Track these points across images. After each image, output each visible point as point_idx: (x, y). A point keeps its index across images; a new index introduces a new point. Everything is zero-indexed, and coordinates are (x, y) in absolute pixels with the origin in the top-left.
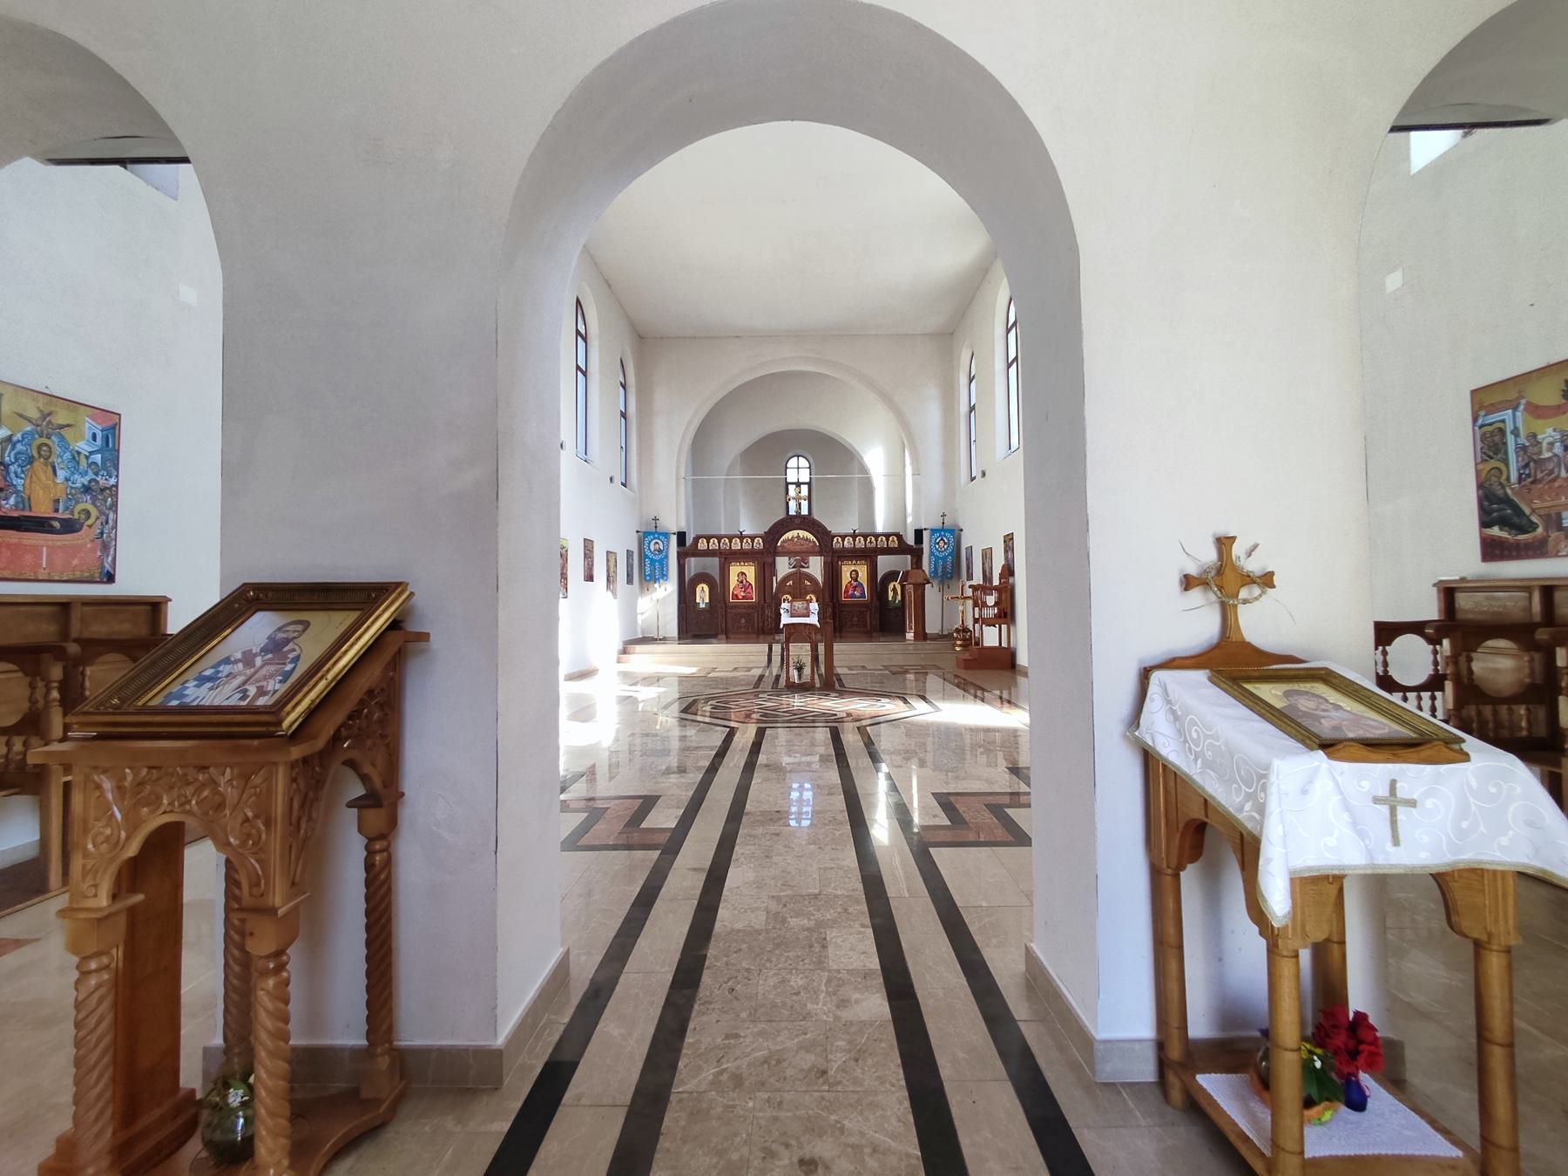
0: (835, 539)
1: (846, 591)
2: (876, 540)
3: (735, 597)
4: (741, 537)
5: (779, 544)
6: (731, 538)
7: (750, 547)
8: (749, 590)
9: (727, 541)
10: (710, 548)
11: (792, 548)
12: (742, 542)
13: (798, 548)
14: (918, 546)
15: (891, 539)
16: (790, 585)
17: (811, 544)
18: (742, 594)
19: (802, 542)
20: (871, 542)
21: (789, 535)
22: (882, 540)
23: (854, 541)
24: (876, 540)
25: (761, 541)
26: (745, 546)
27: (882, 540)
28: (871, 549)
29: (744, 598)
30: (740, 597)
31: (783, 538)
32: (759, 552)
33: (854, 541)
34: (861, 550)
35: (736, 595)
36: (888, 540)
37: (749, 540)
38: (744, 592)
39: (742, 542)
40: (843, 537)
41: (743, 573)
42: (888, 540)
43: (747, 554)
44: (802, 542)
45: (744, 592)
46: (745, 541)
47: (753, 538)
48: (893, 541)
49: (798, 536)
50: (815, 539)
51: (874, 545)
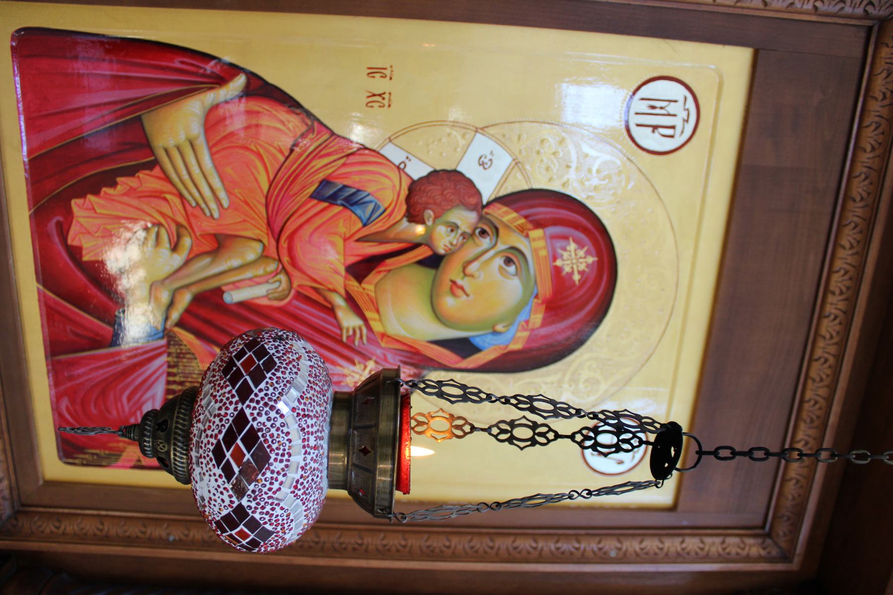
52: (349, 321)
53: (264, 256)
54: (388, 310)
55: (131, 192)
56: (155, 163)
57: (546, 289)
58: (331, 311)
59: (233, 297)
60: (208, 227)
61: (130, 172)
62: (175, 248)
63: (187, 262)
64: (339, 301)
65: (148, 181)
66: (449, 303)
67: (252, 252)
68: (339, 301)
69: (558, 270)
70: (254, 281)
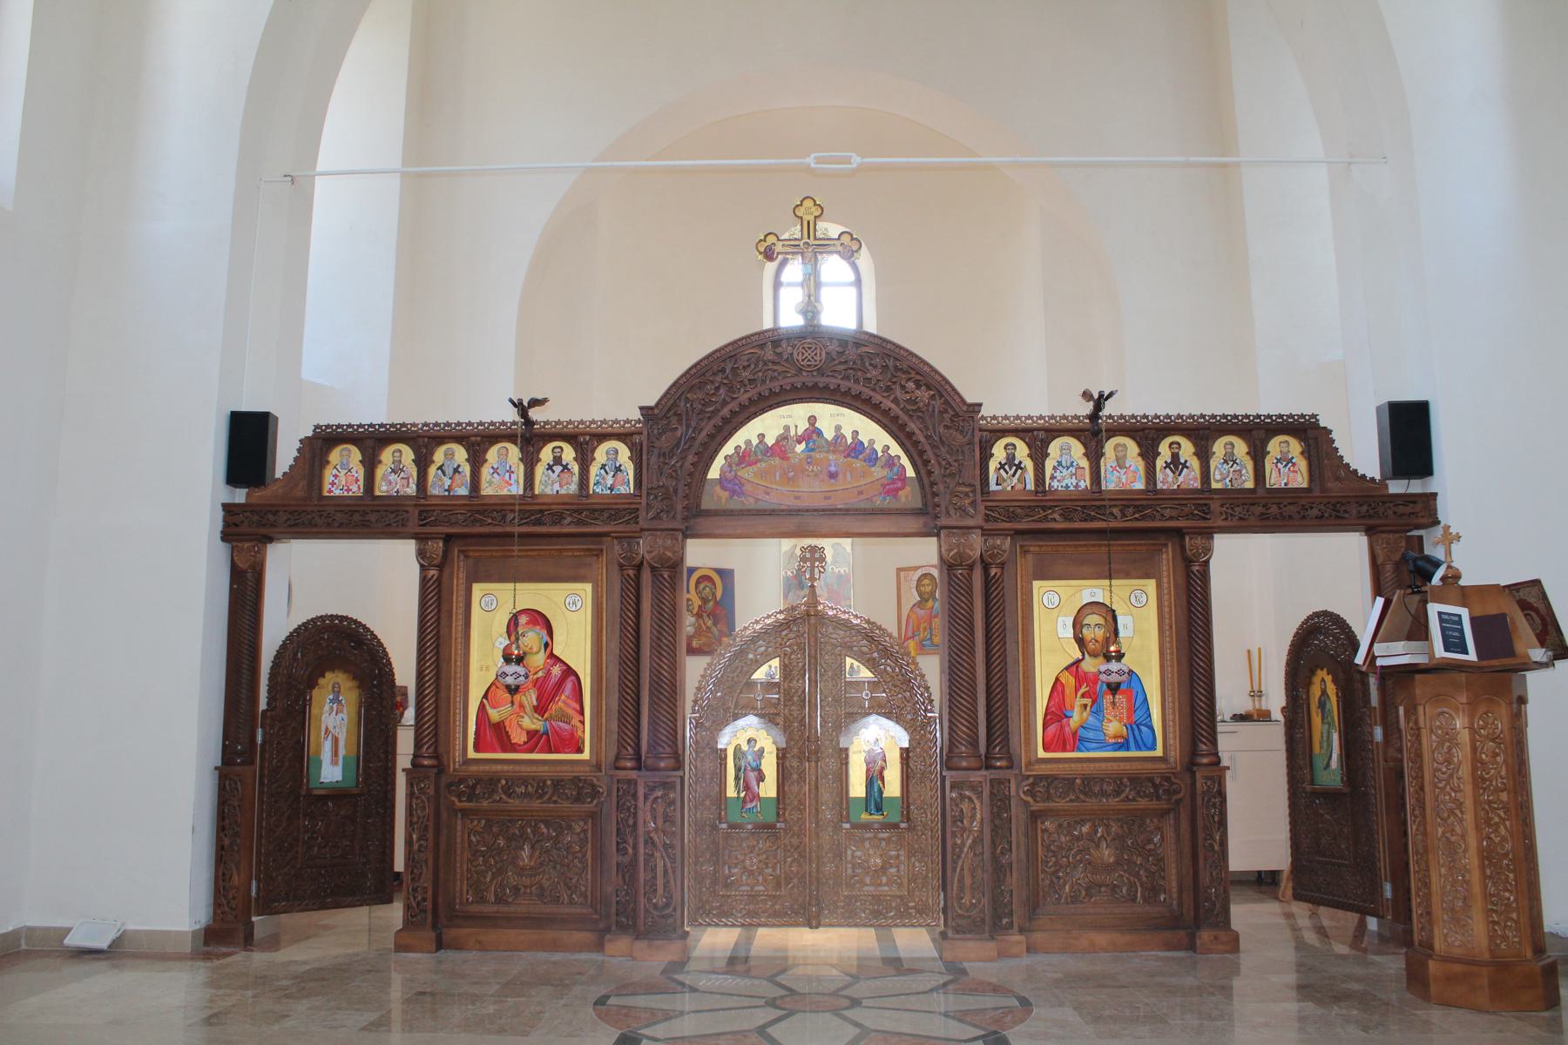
0: (999, 452)
1: (1056, 714)
2: (1204, 455)
3: (494, 734)
4: (530, 437)
5: (714, 473)
6: (478, 441)
7: (573, 488)
8: (563, 702)
9: (460, 454)
10: (381, 489)
11: (779, 495)
12: (530, 461)
13: (811, 491)
14: (1396, 487)
15: (1275, 446)
16: (769, 686)
17: (878, 472)
18: (531, 722)
19: (835, 461)
20: (1176, 464)
21: (767, 426)
22: (1229, 459)
23: (1095, 455)
24: (1204, 455)
25: (624, 453)
26: (548, 483)
27: (1229, 459)
28: (1179, 498)
29: (535, 740)
30: (518, 737)
31: (728, 449)
32: (618, 510)
33: (1095, 455)
34: (1128, 501)
35: (499, 728)
36: (1258, 455)
37: (569, 454)
38: (540, 709)
39: (530, 461)
40: (1039, 436)
41: (540, 620)
42: (1258, 455)
43: (558, 518)
44: (835, 461)
45: (540, 709)
46: (546, 454)
47: (584, 440)
48: (1287, 460)
49: (813, 433)
50: (895, 450)
51: (1191, 478)
52: (540, 674)
53: (525, 695)
54: (536, 665)
55: (510, 727)
56: (503, 721)
57: (531, 626)
58: (538, 679)
59: (535, 703)
60: (518, 709)
61: (505, 728)
62: (523, 717)
63: (526, 713)
64: (535, 677)
65: (507, 724)
66: (535, 650)
67: (524, 698)
68: (535, 677)
69: (526, 623)
70: (531, 698)
